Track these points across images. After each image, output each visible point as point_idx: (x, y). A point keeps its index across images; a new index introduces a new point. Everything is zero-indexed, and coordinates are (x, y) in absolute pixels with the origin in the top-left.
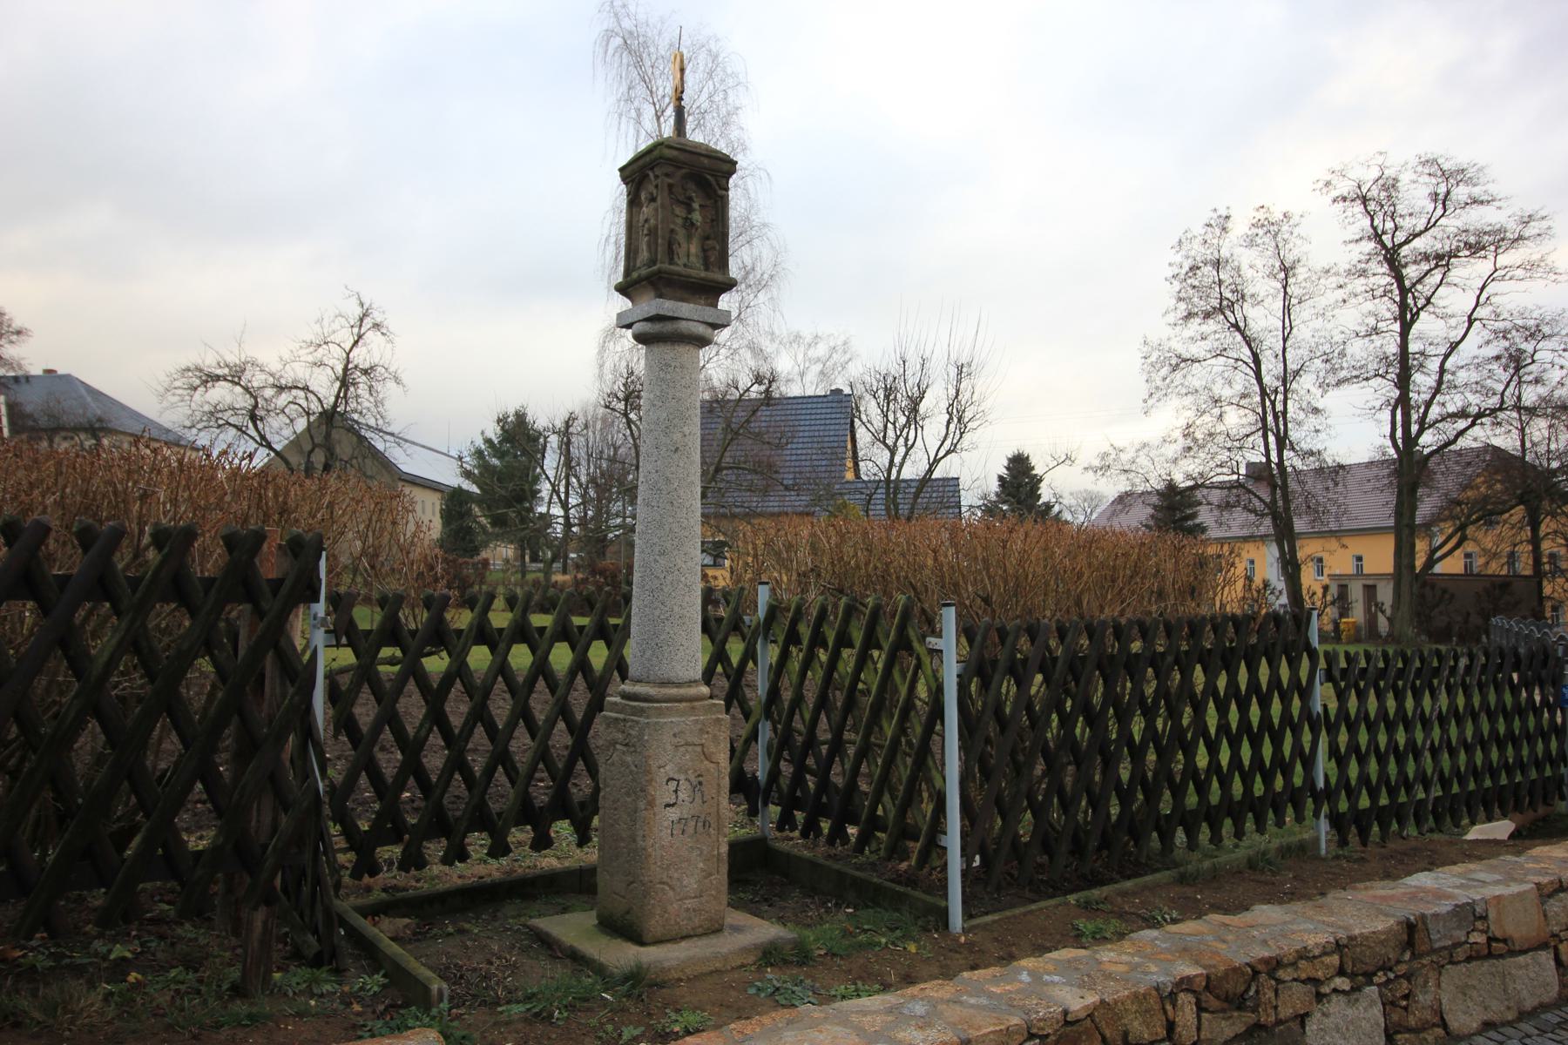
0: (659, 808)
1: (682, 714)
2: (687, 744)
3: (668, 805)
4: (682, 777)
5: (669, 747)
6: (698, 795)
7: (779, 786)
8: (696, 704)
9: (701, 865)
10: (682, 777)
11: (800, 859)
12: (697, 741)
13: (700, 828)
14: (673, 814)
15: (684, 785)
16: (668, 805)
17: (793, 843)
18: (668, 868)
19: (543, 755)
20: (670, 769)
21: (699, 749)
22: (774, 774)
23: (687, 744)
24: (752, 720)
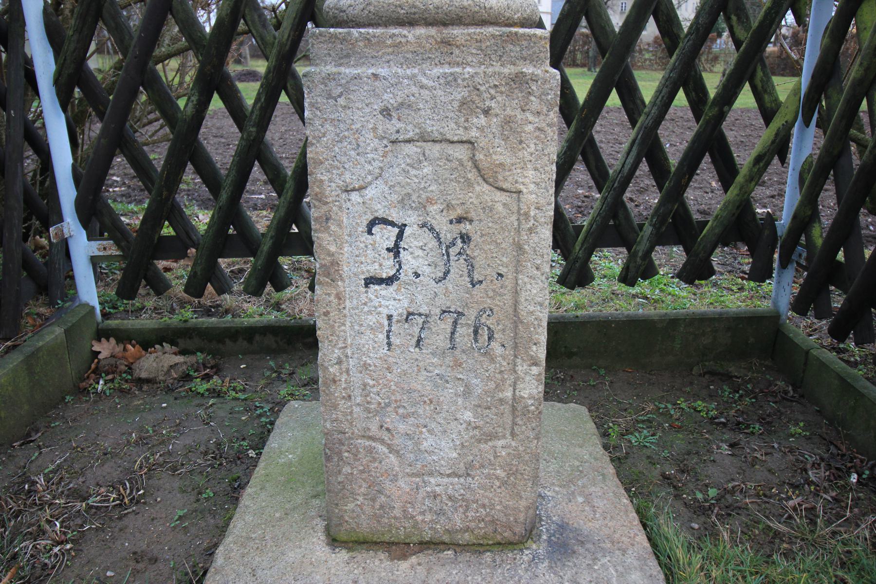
0: (350, 284)
1: (419, 56)
2: (424, 138)
3: (370, 281)
4: (412, 219)
5: (370, 142)
6: (458, 267)
7: (809, 238)
8: (457, 32)
9: (468, 415)
10: (412, 219)
11: (823, 366)
12: (452, 131)
13: (464, 332)
14: (390, 301)
15: (414, 238)
16: (370, 281)
17: (809, 332)
18: (382, 409)
19: (649, 149)
20: (377, 198)
21: (460, 153)
22: (804, 219)
23: (424, 138)
24: (777, 123)
